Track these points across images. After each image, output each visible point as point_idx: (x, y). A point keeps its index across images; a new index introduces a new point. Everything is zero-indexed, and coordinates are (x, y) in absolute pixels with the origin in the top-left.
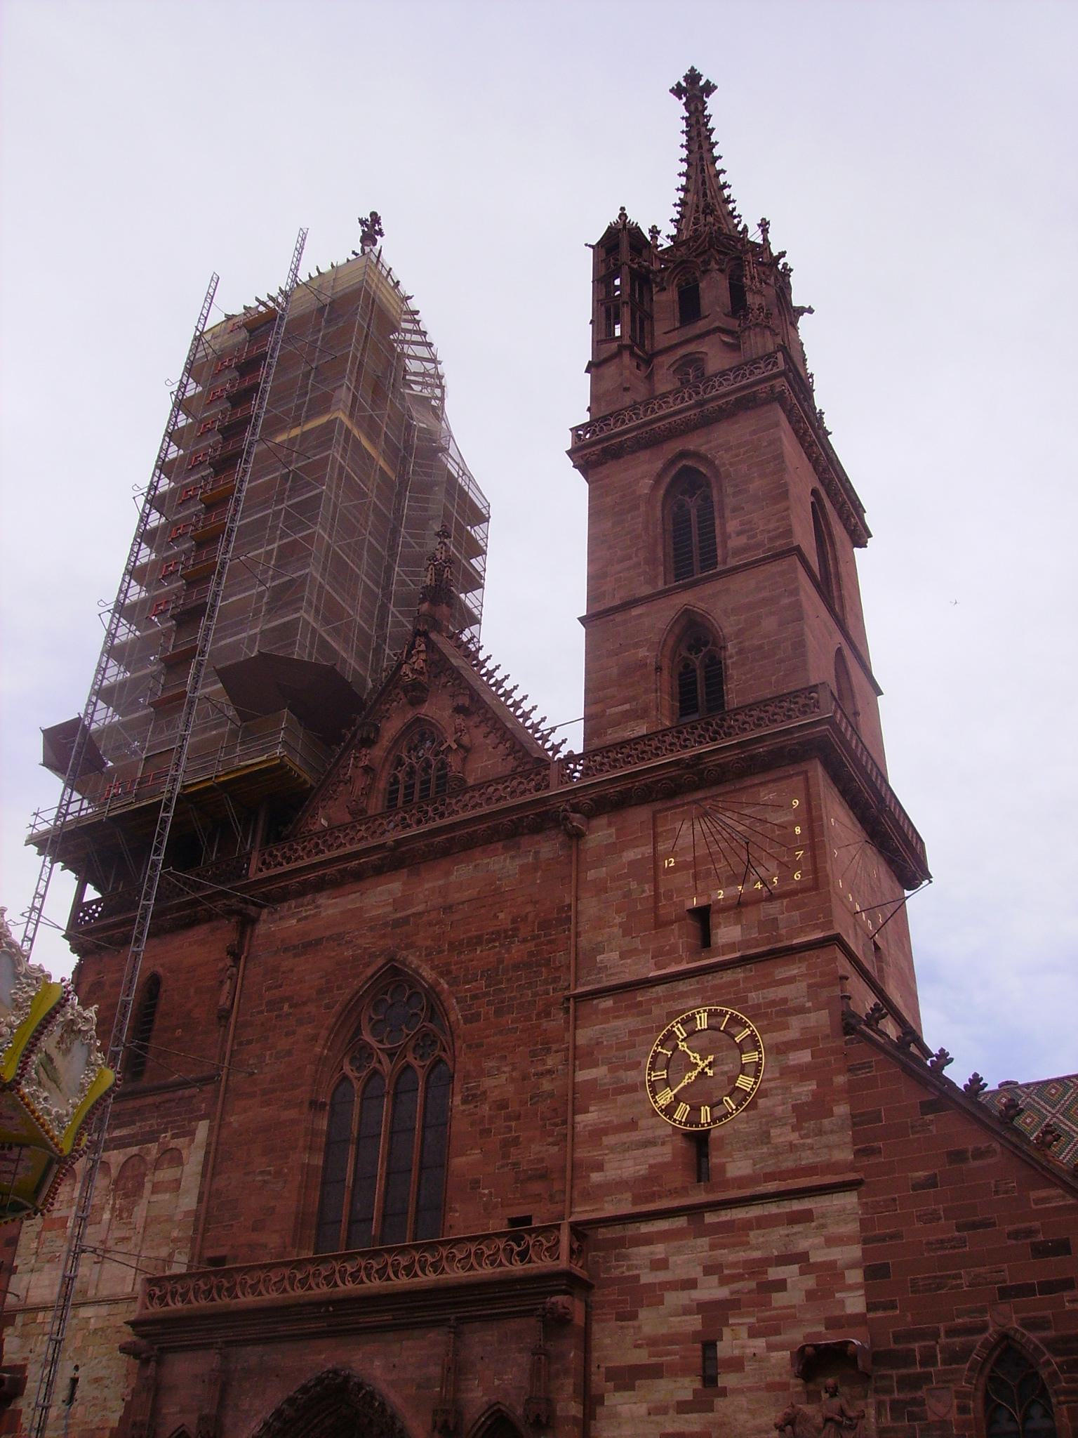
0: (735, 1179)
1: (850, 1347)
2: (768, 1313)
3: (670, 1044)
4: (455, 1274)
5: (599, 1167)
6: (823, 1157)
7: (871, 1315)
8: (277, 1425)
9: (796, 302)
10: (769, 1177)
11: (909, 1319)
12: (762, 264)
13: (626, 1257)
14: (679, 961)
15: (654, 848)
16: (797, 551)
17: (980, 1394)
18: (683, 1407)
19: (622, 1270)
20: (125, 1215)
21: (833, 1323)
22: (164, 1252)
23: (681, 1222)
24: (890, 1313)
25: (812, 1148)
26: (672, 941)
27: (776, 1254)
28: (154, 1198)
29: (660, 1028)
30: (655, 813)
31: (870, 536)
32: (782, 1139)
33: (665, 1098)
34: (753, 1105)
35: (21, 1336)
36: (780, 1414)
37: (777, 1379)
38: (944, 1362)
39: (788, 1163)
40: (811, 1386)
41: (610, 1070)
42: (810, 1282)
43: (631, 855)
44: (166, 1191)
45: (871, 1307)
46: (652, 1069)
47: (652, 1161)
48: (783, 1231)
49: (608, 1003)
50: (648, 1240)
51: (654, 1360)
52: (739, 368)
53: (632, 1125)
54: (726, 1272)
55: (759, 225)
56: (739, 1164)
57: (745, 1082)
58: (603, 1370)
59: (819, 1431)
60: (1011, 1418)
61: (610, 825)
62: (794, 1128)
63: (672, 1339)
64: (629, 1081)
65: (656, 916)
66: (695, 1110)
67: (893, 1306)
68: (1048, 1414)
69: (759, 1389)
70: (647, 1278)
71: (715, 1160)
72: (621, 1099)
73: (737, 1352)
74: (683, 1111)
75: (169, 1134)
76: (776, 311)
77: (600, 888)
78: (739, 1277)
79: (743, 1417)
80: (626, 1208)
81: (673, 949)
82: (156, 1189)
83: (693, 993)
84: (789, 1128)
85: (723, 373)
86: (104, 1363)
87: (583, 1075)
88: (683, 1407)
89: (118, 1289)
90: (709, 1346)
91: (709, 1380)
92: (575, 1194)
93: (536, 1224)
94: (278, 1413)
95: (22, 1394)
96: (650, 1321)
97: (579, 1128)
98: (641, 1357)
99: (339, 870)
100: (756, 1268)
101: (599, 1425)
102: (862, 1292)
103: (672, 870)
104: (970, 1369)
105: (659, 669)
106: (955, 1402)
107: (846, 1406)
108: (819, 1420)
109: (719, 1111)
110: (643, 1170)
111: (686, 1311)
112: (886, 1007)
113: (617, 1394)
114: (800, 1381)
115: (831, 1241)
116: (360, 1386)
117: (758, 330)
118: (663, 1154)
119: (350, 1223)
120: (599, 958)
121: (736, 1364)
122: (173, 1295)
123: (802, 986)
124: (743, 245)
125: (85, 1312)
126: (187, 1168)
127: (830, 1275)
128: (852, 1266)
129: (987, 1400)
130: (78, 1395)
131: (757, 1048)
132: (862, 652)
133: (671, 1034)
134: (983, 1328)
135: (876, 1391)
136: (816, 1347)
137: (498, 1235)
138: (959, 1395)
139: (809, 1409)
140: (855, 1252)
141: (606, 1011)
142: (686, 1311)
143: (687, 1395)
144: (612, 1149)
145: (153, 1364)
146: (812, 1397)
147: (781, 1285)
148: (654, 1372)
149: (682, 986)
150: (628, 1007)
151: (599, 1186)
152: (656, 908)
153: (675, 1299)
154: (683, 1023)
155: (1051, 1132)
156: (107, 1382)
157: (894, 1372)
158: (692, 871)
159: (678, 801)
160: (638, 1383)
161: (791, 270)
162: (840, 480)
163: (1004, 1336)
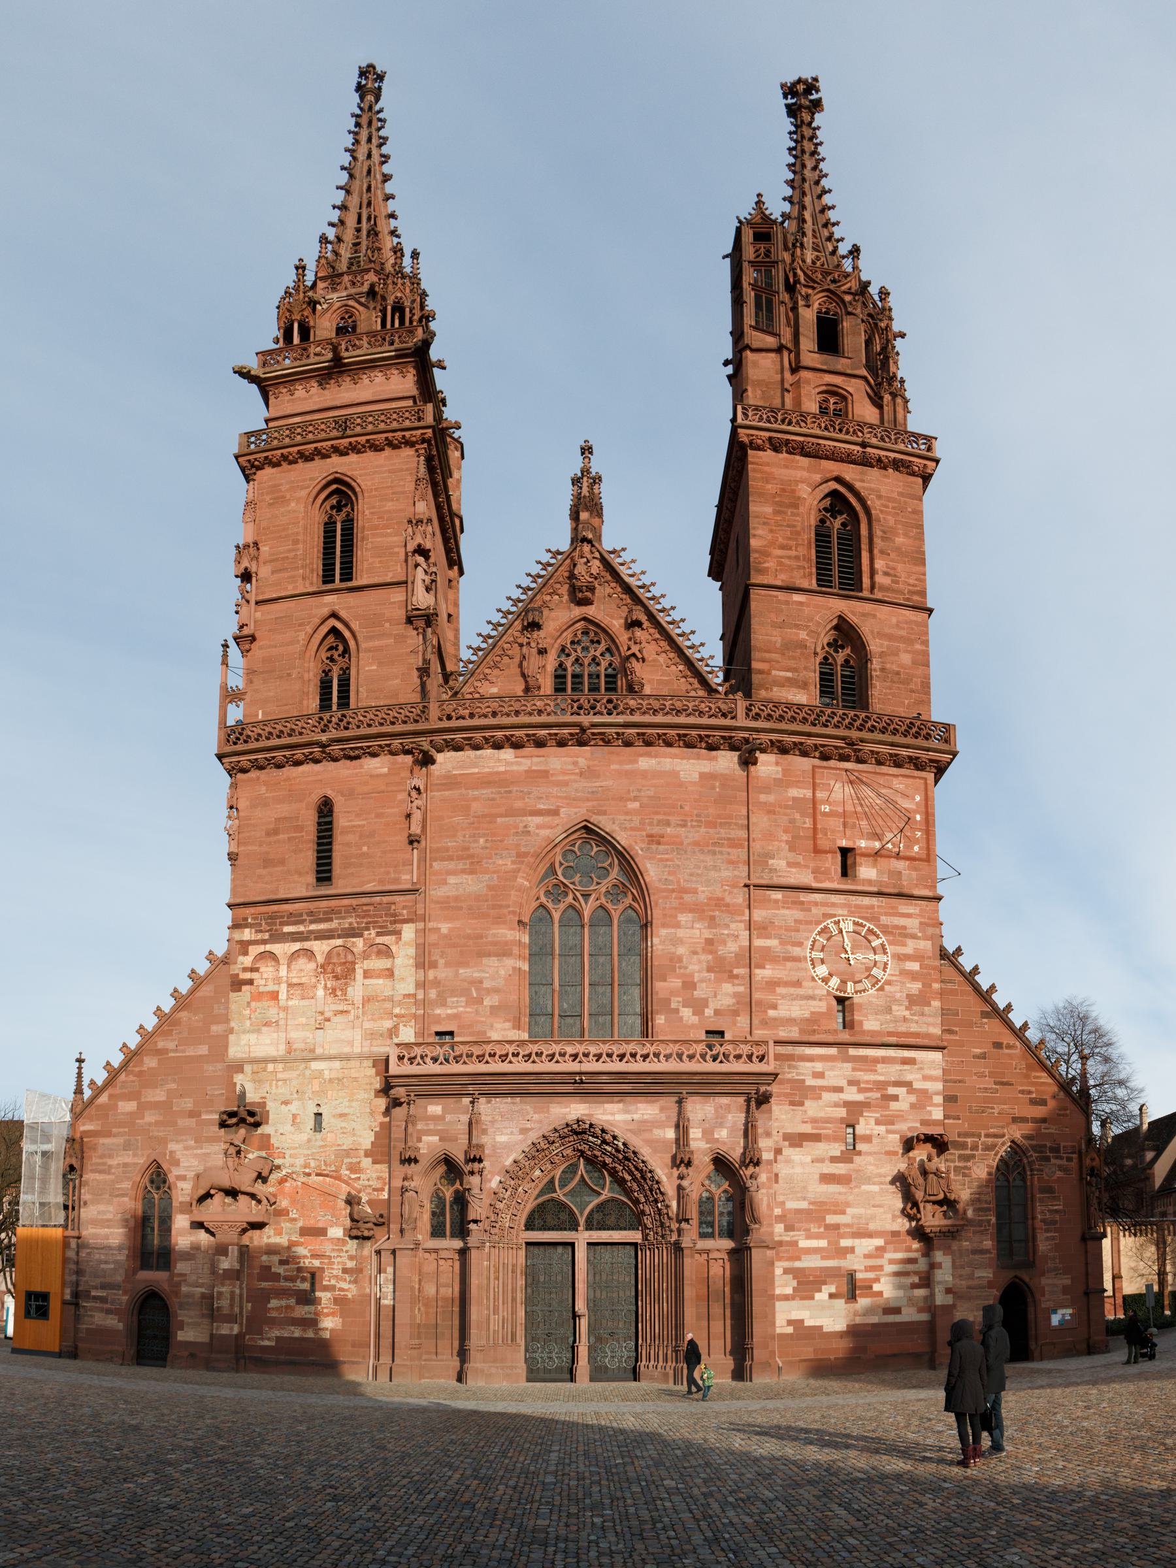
0: (869, 1031)
5: (775, 1007)
13: (795, 1067)
18: (834, 1160)
20: (339, 993)
23: (833, 1051)
28: (367, 982)
29: (819, 923)
33: (822, 971)
41: (781, 943)
44: (379, 977)
49: (777, 895)
50: (811, 1059)
51: (814, 1131)
53: (798, 984)
63: (827, 1120)
64: (795, 954)
66: (844, 982)
70: (810, 1082)
72: (789, 964)
73: (868, 1132)
74: (835, 982)
75: (373, 932)
78: (870, 1090)
79: (871, 1168)
82: (367, 974)
87: (758, 943)
88: (834, 1160)
89: (347, 1050)
95: (267, 1123)
96: (812, 1108)
98: (807, 1129)
99: (527, 735)
100: (881, 1086)
109: (859, 987)
110: (807, 1015)
111: (836, 1105)
118: (821, 1006)
120: (771, 862)
121: (868, 1139)
125: (315, 1065)
126: (398, 961)
138: (988, 1166)
141: (776, 901)
142: (836, 1105)
143: (838, 1154)
144: (783, 997)
148: (816, 1138)
150: (794, 903)
151: (775, 1019)
153: (828, 1097)
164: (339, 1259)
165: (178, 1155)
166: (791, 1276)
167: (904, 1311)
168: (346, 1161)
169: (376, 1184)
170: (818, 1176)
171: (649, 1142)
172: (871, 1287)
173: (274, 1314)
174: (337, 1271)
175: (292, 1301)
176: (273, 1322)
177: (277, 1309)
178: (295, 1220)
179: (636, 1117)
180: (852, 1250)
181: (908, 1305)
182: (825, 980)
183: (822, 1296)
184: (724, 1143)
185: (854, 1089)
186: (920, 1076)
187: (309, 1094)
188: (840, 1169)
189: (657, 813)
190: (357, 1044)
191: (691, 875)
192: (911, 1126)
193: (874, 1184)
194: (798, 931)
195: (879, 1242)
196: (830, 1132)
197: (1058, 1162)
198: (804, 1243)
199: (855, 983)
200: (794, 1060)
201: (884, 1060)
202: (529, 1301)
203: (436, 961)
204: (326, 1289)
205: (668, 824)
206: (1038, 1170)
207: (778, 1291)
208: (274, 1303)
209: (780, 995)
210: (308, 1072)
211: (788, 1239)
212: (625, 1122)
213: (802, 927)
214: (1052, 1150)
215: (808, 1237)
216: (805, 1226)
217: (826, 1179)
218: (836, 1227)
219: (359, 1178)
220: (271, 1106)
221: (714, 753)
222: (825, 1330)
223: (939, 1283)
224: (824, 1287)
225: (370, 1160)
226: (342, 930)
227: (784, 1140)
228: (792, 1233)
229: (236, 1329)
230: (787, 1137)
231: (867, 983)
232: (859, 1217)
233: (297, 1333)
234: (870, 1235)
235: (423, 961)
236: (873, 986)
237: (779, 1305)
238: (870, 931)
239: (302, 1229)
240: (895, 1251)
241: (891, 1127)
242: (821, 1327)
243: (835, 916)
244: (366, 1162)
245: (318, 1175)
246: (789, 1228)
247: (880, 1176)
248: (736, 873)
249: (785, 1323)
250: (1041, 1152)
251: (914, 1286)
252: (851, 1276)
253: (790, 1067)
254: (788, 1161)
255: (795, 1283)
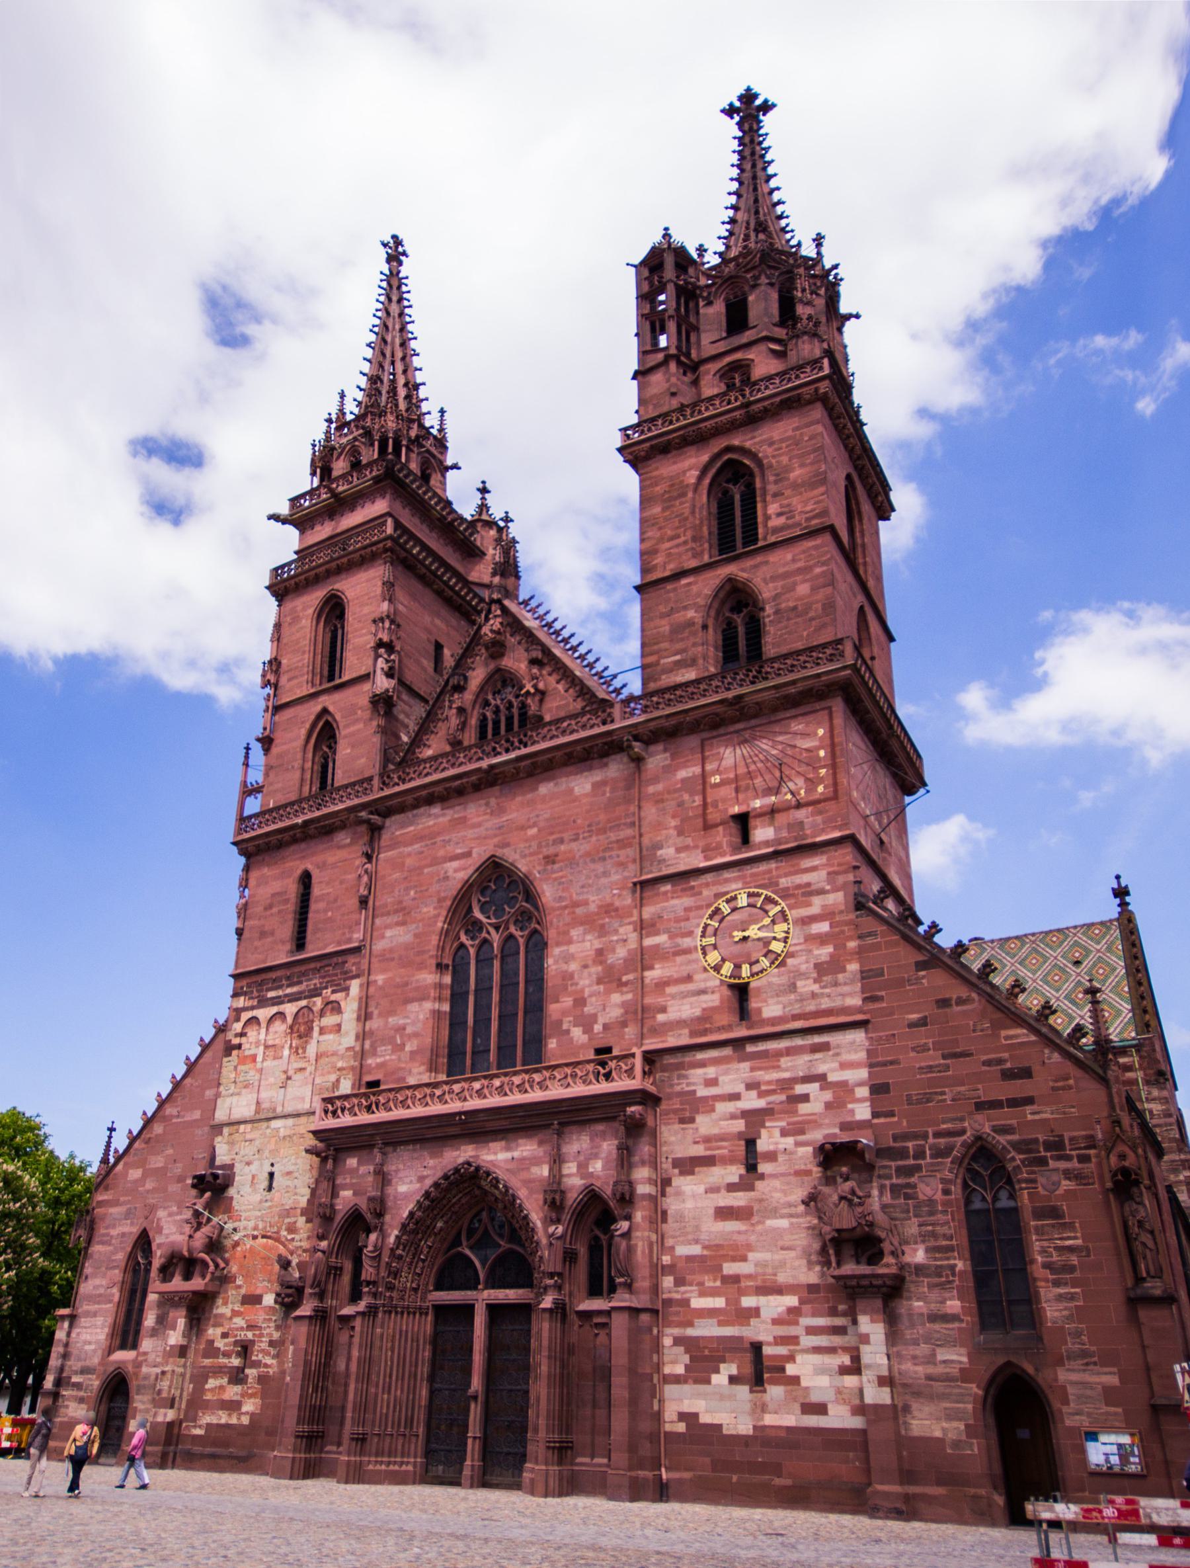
1: (859, 1145)
2: (795, 1119)
3: (717, 917)
4: (556, 1092)
5: (664, 1010)
6: (838, 1003)
7: (876, 1121)
8: (427, 1203)
9: (844, 308)
10: (795, 1017)
11: (905, 1124)
12: (814, 276)
13: (686, 1077)
14: (723, 855)
15: (703, 767)
16: (832, 529)
17: (959, 1181)
18: (731, 1187)
19: (682, 1086)
21: (845, 1127)
22: (333, 1078)
23: (727, 1051)
24: (888, 1120)
25: (829, 996)
26: (718, 839)
27: (801, 1074)
30: (703, 741)
31: (893, 510)
32: (806, 989)
33: (714, 957)
34: (783, 964)
35: (228, 1143)
36: (805, 1193)
37: (803, 1167)
38: (932, 1157)
39: (811, 1007)
40: (829, 1173)
41: (671, 938)
42: (828, 1096)
43: (682, 774)
45: (875, 1115)
46: (703, 936)
47: (705, 1006)
48: (807, 1057)
49: (668, 887)
50: (703, 1064)
51: (708, 1153)
52: (784, 373)
53: (689, 978)
54: (763, 1088)
55: (814, 240)
56: (773, 1007)
57: (776, 947)
58: (670, 1160)
59: (837, 1206)
60: (984, 1199)
61: (665, 750)
62: (816, 981)
63: (722, 1138)
65: (705, 821)
66: (738, 967)
67: (891, 1114)
68: (1012, 1196)
69: (790, 1174)
70: (702, 1092)
71: (753, 1004)
72: (679, 959)
73: (772, 1148)
74: (727, 968)
76: (823, 319)
77: (659, 800)
79: (777, 1195)
80: (684, 1039)
81: (719, 846)
83: (735, 879)
84: (811, 981)
85: (770, 378)
86: (293, 1161)
87: (648, 942)
88: (731, 1187)
90: (751, 1143)
91: (751, 1168)
92: (645, 1030)
93: (615, 1052)
94: (427, 1195)
96: (705, 1124)
97: (647, 981)
98: (699, 1150)
100: (785, 1085)
101: (668, 1200)
102: (868, 1104)
103: (716, 785)
104: (952, 1162)
105: (705, 627)
106: (940, 1186)
107: (857, 1189)
108: (835, 1198)
109: (756, 968)
110: (697, 1012)
111: (733, 1117)
112: (889, 889)
113: (682, 1178)
114: (820, 1169)
115: (844, 1066)
116: (488, 1174)
117: (806, 338)
118: (713, 1000)
119: (474, 1053)
120: (659, 853)
121: (772, 1156)
122: (343, 1110)
123: (823, 874)
124: (796, 260)
125: (275, 1124)
127: (843, 1091)
128: (860, 1084)
129: (965, 1185)
130: (275, 1184)
131: (786, 920)
132: (880, 607)
133: (717, 910)
134: (963, 1132)
135: (880, 1177)
136: (833, 1144)
137: (589, 1062)
138: (943, 1181)
139: (826, 1190)
140: (863, 1074)
141: (666, 893)
142: (733, 1117)
143: (735, 1179)
144: (673, 997)
145: (330, 1161)
146: (829, 1181)
147: (805, 1098)
148: (708, 1161)
149: (727, 875)
150: (684, 890)
151: (664, 1024)
152: (704, 815)
153: (723, 1108)
154: (728, 901)
155: (1018, 986)
156: (296, 1174)
157: (893, 1164)
158: (734, 786)
159: (722, 731)
160: (697, 1169)
161: (841, 280)
162: (872, 465)
163: (978, 1138)
164: (268, 1331)
165: (163, 1223)
166: (682, 1349)
167: (831, 1409)
168: (287, 1220)
169: (305, 1244)
170: (711, 1211)
171: (527, 1182)
172: (783, 1369)
173: (208, 1396)
174: (264, 1346)
175: (224, 1381)
176: (206, 1406)
177: (212, 1390)
178: (239, 1287)
179: (516, 1154)
180: (755, 1312)
181: (837, 1401)
182: (717, 968)
183: (720, 1379)
184: (598, 1178)
185: (754, 1093)
186: (836, 1065)
187: (266, 1153)
188: (739, 1199)
189: (552, 833)
190: (308, 1100)
191: (583, 887)
192: (828, 1131)
193: (782, 1217)
194: (688, 919)
195: (792, 1301)
196: (725, 1151)
197: (1063, 1165)
198: (697, 1303)
199: (751, 964)
200: (683, 1069)
201: (789, 1052)
202: (432, 1378)
203: (372, 1013)
204: (256, 1364)
205: (562, 841)
206: (1027, 1181)
207: (667, 1370)
208: (212, 1383)
209: (670, 995)
210: (268, 1131)
211: (677, 1296)
212: (506, 1161)
213: (692, 914)
214: (1048, 1146)
215: (703, 1294)
216: (698, 1278)
217: (724, 1213)
218: (736, 1279)
219: (293, 1239)
220: (237, 1169)
221: (605, 760)
222: (725, 1432)
223: (869, 1366)
224: (722, 1366)
225: (304, 1219)
226: (309, 991)
227: (674, 1167)
228: (683, 1289)
229: (171, 1415)
230: (677, 1163)
231: (765, 963)
232: (764, 1264)
233: (223, 1418)
234: (779, 1290)
235: (364, 1016)
236: (772, 963)
237: (670, 1390)
238: (768, 900)
239: (244, 1297)
240: (814, 1315)
241: (801, 1138)
242: (720, 1426)
243: (727, 893)
244: (301, 1220)
245: (264, 1237)
246: (680, 1282)
247: (790, 1205)
248: (626, 874)
249: (675, 1418)
250: (1029, 1151)
251: (844, 1371)
252: (757, 1347)
253: (679, 1077)
254: (679, 1193)
255: (686, 1359)
